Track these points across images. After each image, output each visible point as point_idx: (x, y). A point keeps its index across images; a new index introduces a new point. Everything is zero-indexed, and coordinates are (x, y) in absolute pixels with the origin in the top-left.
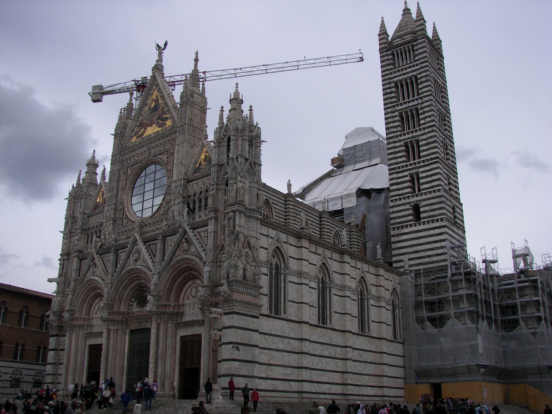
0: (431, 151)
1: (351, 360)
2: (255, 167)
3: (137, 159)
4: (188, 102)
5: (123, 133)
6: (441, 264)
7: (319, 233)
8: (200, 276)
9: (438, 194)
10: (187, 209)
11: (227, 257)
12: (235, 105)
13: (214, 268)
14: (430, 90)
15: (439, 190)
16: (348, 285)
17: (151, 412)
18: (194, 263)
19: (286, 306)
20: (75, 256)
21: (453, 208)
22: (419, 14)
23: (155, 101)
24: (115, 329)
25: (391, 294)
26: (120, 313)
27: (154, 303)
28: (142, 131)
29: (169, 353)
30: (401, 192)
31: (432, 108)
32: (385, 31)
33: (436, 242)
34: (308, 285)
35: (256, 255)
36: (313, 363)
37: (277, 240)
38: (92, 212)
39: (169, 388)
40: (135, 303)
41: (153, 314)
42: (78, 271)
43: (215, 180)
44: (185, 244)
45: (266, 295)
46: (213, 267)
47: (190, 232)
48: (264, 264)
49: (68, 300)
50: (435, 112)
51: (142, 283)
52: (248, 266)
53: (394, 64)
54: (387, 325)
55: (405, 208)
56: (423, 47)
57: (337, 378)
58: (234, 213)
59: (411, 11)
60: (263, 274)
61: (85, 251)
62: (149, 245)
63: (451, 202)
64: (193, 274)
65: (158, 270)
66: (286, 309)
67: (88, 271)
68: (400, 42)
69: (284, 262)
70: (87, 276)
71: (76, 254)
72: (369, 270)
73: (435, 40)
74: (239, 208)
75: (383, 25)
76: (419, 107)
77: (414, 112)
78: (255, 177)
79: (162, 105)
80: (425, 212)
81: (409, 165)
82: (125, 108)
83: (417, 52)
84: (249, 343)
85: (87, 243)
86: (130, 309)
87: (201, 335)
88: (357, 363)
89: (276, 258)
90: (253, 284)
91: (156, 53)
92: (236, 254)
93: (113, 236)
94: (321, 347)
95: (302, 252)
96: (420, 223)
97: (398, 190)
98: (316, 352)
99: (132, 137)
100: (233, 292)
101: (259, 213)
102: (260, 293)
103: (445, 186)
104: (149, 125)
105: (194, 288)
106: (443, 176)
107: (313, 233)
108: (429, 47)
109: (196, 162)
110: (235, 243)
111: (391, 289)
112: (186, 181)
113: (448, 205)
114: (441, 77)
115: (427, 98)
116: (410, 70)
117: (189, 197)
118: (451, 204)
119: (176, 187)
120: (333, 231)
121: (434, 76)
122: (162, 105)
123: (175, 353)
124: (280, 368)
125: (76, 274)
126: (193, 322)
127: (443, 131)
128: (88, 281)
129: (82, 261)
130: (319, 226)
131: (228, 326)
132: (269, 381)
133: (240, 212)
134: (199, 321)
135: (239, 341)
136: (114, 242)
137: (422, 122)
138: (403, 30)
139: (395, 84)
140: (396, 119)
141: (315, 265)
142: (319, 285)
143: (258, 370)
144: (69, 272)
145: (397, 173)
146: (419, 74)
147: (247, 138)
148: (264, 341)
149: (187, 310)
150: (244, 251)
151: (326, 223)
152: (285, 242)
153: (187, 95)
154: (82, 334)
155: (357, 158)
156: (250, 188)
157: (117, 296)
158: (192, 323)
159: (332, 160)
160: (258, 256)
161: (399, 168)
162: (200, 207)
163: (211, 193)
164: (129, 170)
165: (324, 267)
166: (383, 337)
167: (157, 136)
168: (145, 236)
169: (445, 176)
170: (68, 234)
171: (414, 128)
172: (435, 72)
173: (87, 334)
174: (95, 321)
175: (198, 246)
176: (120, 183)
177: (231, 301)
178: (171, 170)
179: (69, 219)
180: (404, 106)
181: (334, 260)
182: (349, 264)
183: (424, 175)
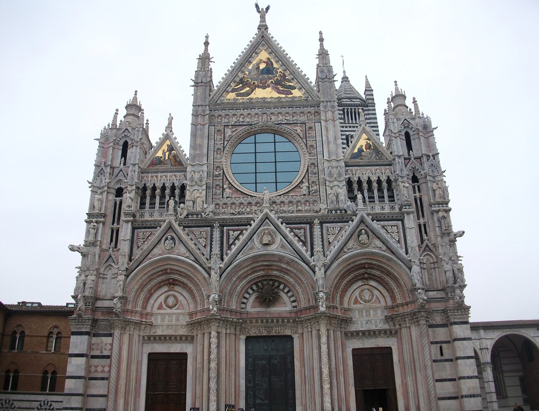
3: (241, 120)
20: (127, 222)
26: (231, 311)
38: (148, 166)
51: (268, 276)
53: (344, 119)
64: (368, 274)
79: (280, 70)
86: (242, 308)
87: (390, 348)
99: (228, 92)
104: (259, 87)
129: (136, 231)
131: (463, 337)
136: (211, 214)
138: (350, 94)
149: (357, 317)
164: (229, 132)
176: (212, 143)
178: (312, 146)
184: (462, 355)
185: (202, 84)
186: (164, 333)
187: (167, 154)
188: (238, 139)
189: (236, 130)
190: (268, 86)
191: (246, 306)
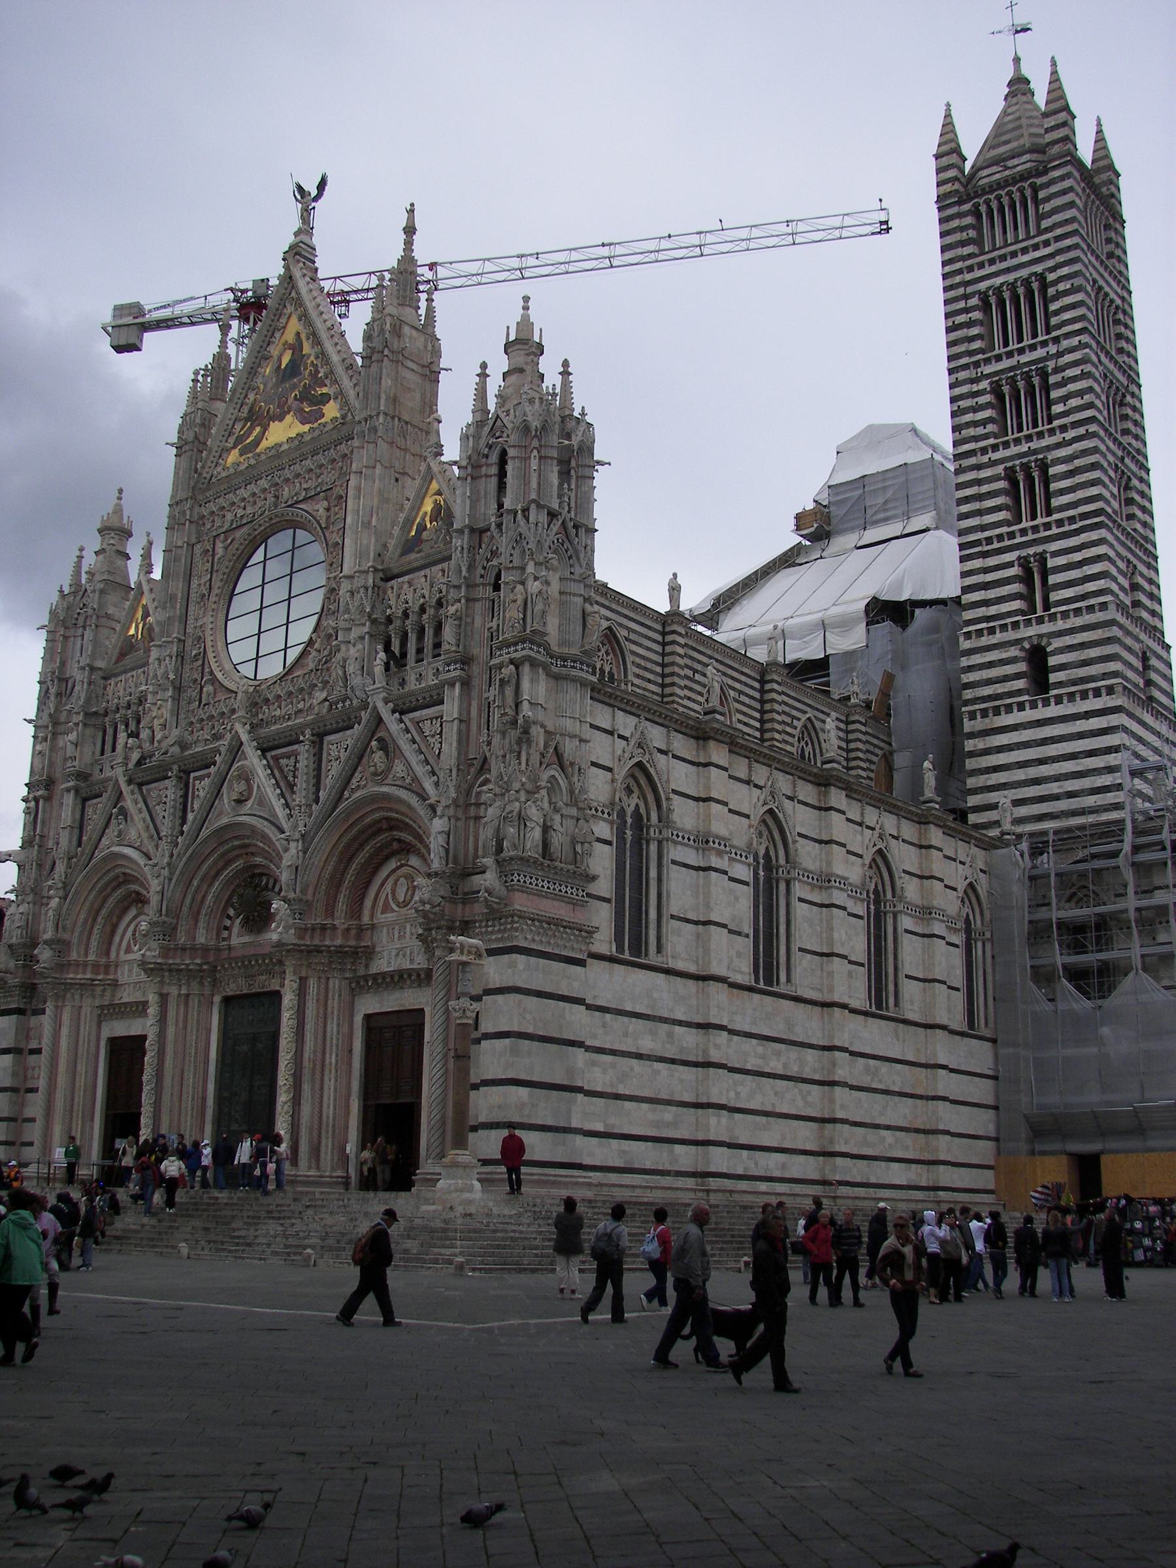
0: (1081, 494)
1: (844, 1084)
2: (577, 535)
3: (240, 512)
4: (386, 353)
5: (202, 439)
6: (1105, 817)
7: (758, 725)
8: (419, 845)
9: (1099, 616)
10: (382, 655)
11: (498, 790)
12: (520, 360)
13: (459, 823)
14: (1082, 318)
15: (1103, 606)
16: (840, 873)
17: (282, 1225)
18: (403, 809)
19: (664, 930)
20: (68, 790)
21: (1145, 659)
22: (1054, 95)
23: (291, 347)
24: (180, 995)
25: (962, 901)
26: (194, 949)
27: (291, 921)
28: (255, 433)
29: (333, 1060)
30: (993, 610)
31: (1088, 368)
32: (953, 145)
33: (1091, 753)
34: (725, 873)
35: (578, 786)
36: (738, 1094)
37: (640, 746)
38: (117, 661)
39: (332, 1160)
40: (238, 921)
41: (288, 951)
42: (76, 831)
43: (464, 573)
44: (378, 756)
45: (608, 901)
46: (457, 819)
47: (392, 723)
48: (603, 812)
49: (51, 913)
50: (1096, 380)
52: (557, 818)
53: (978, 242)
54: (950, 987)
55: (1004, 655)
56: (1064, 192)
57: (804, 1135)
58: (517, 668)
59: (1032, 86)
60: (599, 840)
61: (97, 776)
62: (276, 759)
63: (1138, 640)
64: (399, 841)
65: (301, 828)
66: (664, 941)
67: (103, 833)
68: (997, 176)
69: (659, 806)
70: (101, 846)
71: (71, 784)
72: (899, 831)
73: (1098, 171)
74: (532, 654)
75: (948, 128)
76: (1051, 365)
77: (1036, 381)
78: (577, 566)
79: (312, 358)
80: (1062, 667)
81: (1018, 534)
82: (206, 369)
83: (1047, 207)
84: (558, 1036)
85: (102, 753)
86: (224, 939)
87: (422, 1010)
88: (862, 1094)
89: (635, 795)
90: (571, 867)
91: (295, 208)
92: (523, 784)
93: (176, 732)
94: (760, 1050)
95: (709, 778)
96: (1048, 698)
97: (986, 603)
98: (746, 1062)
99: (229, 450)
100: (513, 890)
101: (588, 666)
102: (589, 895)
103: (1122, 595)
104: (275, 418)
105: (402, 880)
106: (1117, 567)
107: (740, 726)
108: (1084, 190)
109: (409, 522)
110: (519, 753)
111: (961, 886)
112: (381, 575)
113: (1129, 649)
114: (1115, 278)
115: (1074, 341)
116: (1025, 258)
117: (389, 620)
118: (1136, 647)
119: (352, 593)
120: (799, 719)
121: (1095, 275)
122: (312, 358)
123: (350, 1064)
124: (645, 1106)
125: (70, 841)
126: (401, 976)
127: (1119, 436)
128: (105, 859)
130: (758, 706)
132: (614, 1143)
133: (534, 663)
134: (417, 972)
135: (530, 1030)
136: (176, 750)
137: (1057, 409)
139: (980, 299)
140: (982, 400)
141: (748, 817)
142: (756, 874)
143: (584, 1114)
144: (52, 833)
145: (985, 555)
146: (1053, 269)
147: (554, 453)
148: (601, 1031)
149: (384, 941)
150: (545, 776)
151: (779, 698)
152: (660, 751)
153: (382, 330)
154: (88, 1007)
155: (869, 512)
156: (564, 597)
157: (188, 901)
158: (396, 978)
159: (799, 517)
160: (583, 790)
161: (989, 540)
162: (420, 651)
163: (452, 609)
164: (220, 546)
165: (772, 821)
166: (938, 1021)
167: (298, 448)
168: (263, 732)
169: (1122, 565)
170: (47, 727)
171: (1035, 425)
172: (1097, 265)
173: (102, 1007)
174: (126, 971)
175: (414, 759)
176: (195, 582)
177: (507, 917)
178: (337, 544)
179: (49, 683)
180: (1005, 364)
181: (800, 802)
182: (844, 813)
183: (1061, 561)
184: (491, 1030)
185: (187, 448)
186: (131, 999)
187: (141, 626)
188: (235, 562)
189: (233, 540)
190: (289, 412)
191: (230, 935)
